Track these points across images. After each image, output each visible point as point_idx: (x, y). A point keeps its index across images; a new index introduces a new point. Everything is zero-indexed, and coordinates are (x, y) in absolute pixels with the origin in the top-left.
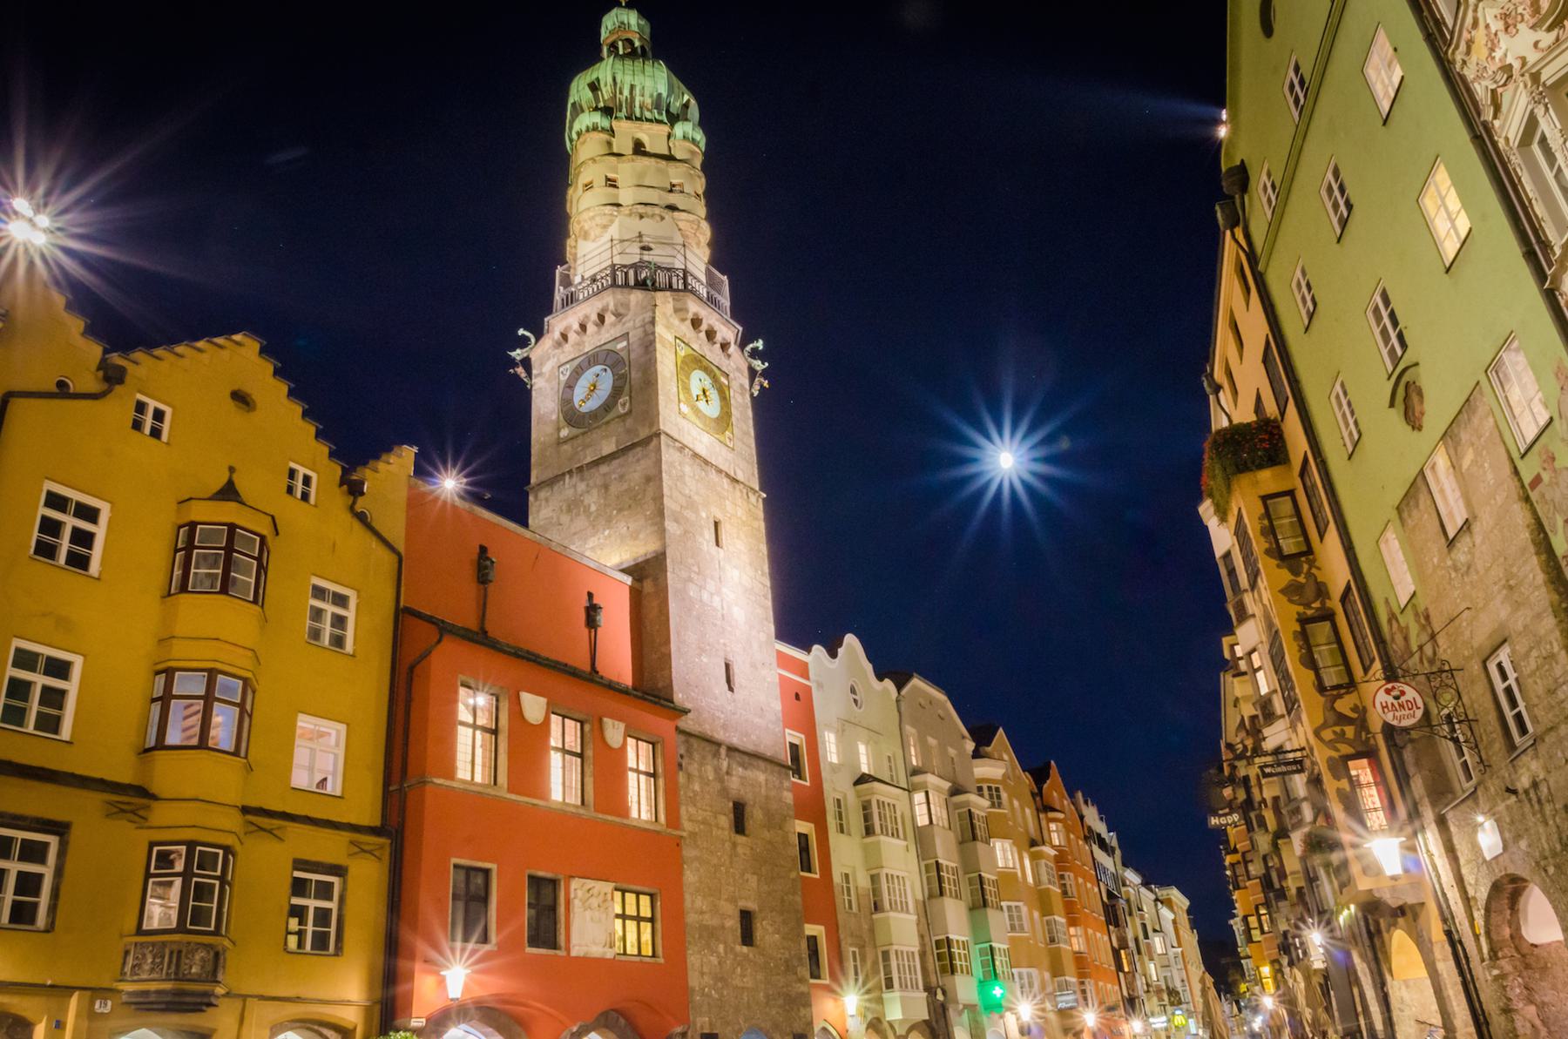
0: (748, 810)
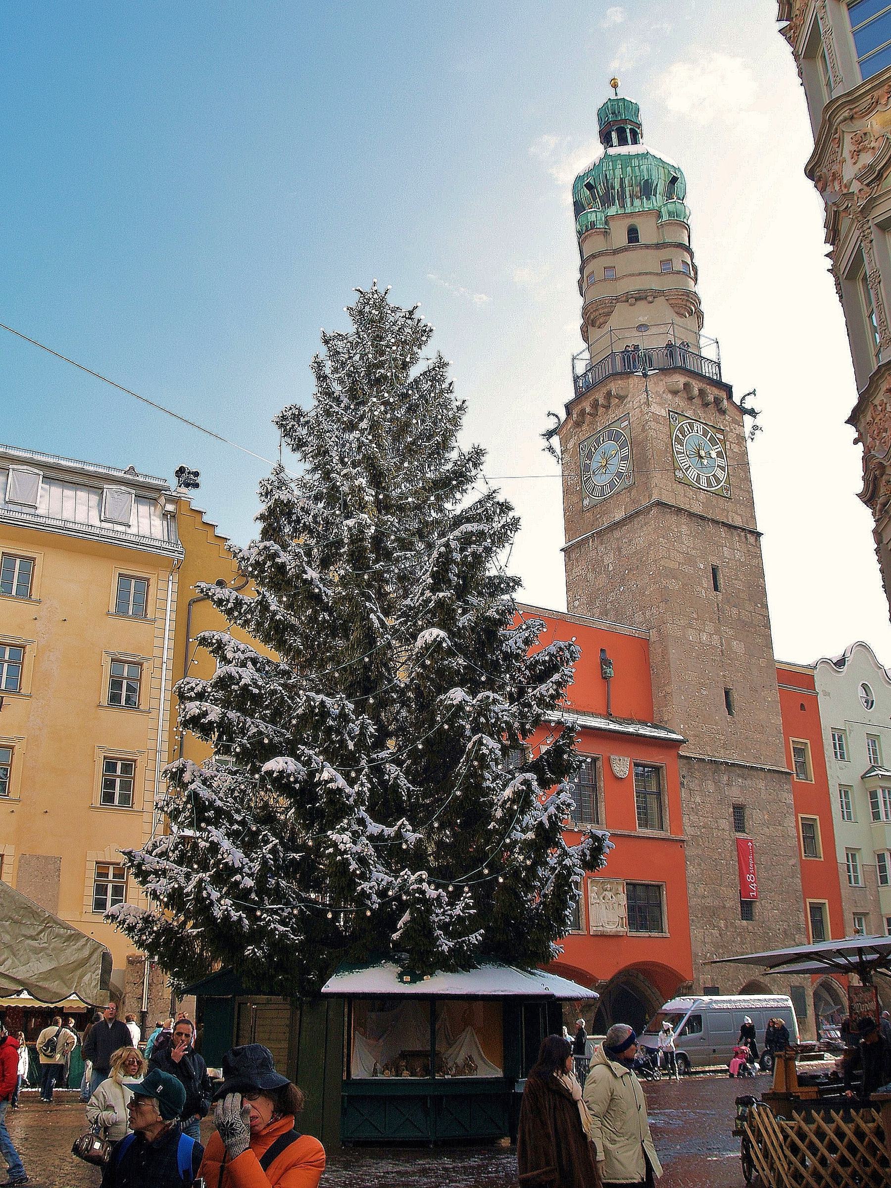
0: (747, 812)
